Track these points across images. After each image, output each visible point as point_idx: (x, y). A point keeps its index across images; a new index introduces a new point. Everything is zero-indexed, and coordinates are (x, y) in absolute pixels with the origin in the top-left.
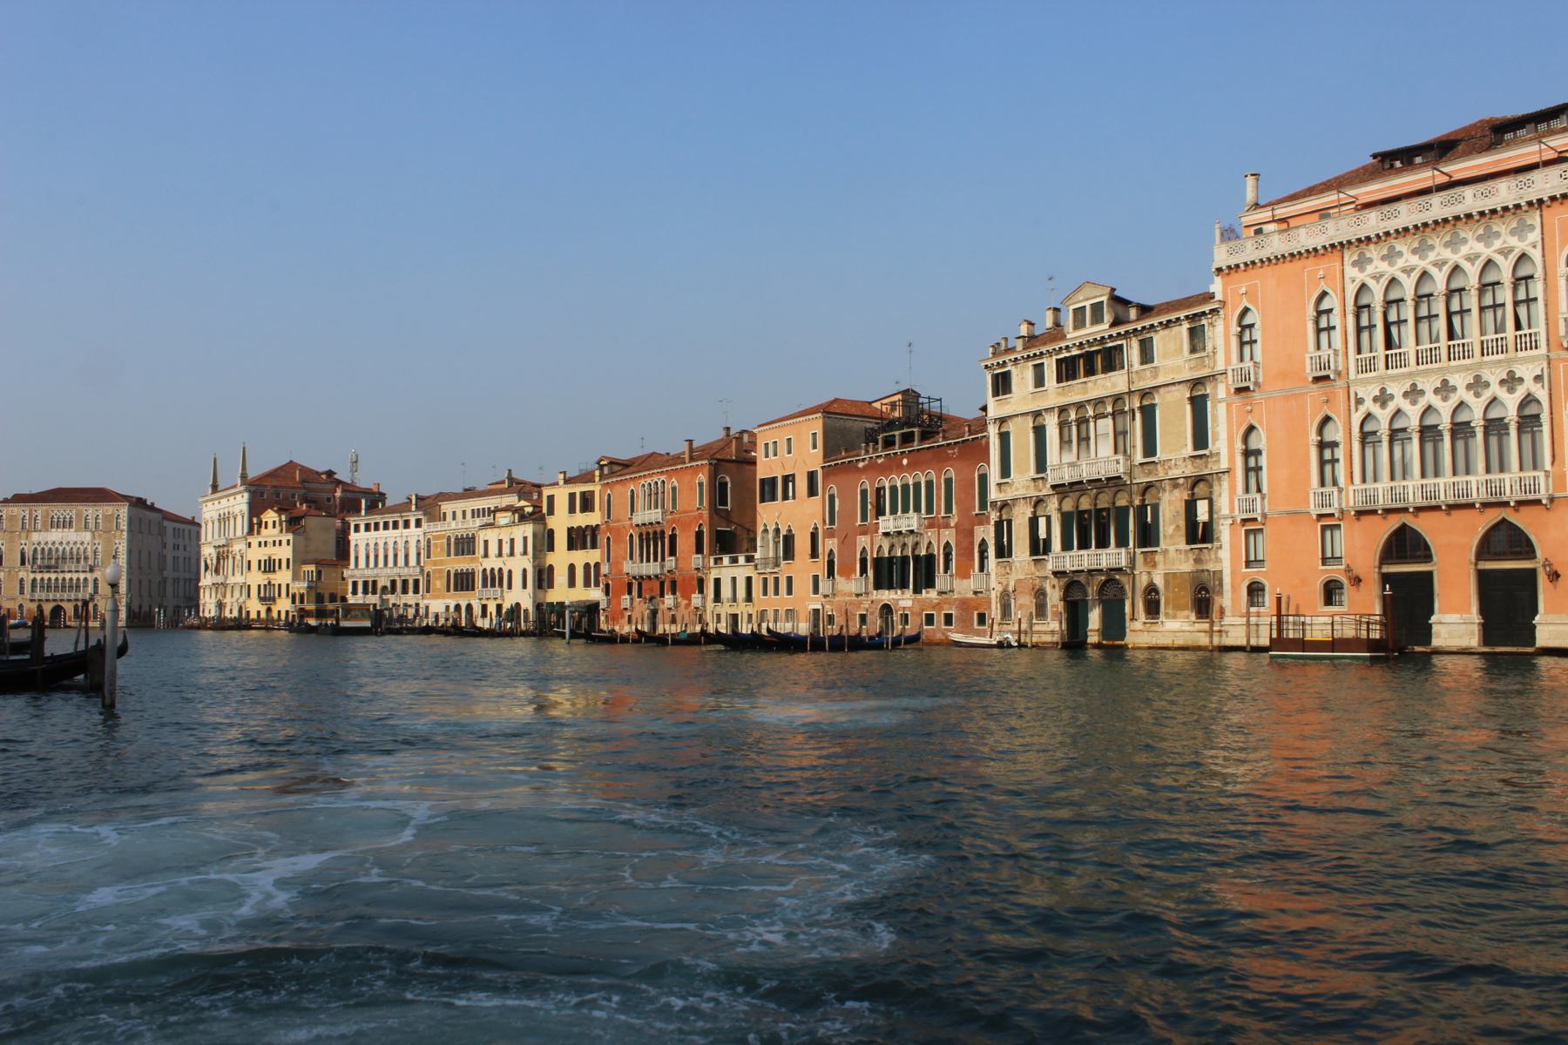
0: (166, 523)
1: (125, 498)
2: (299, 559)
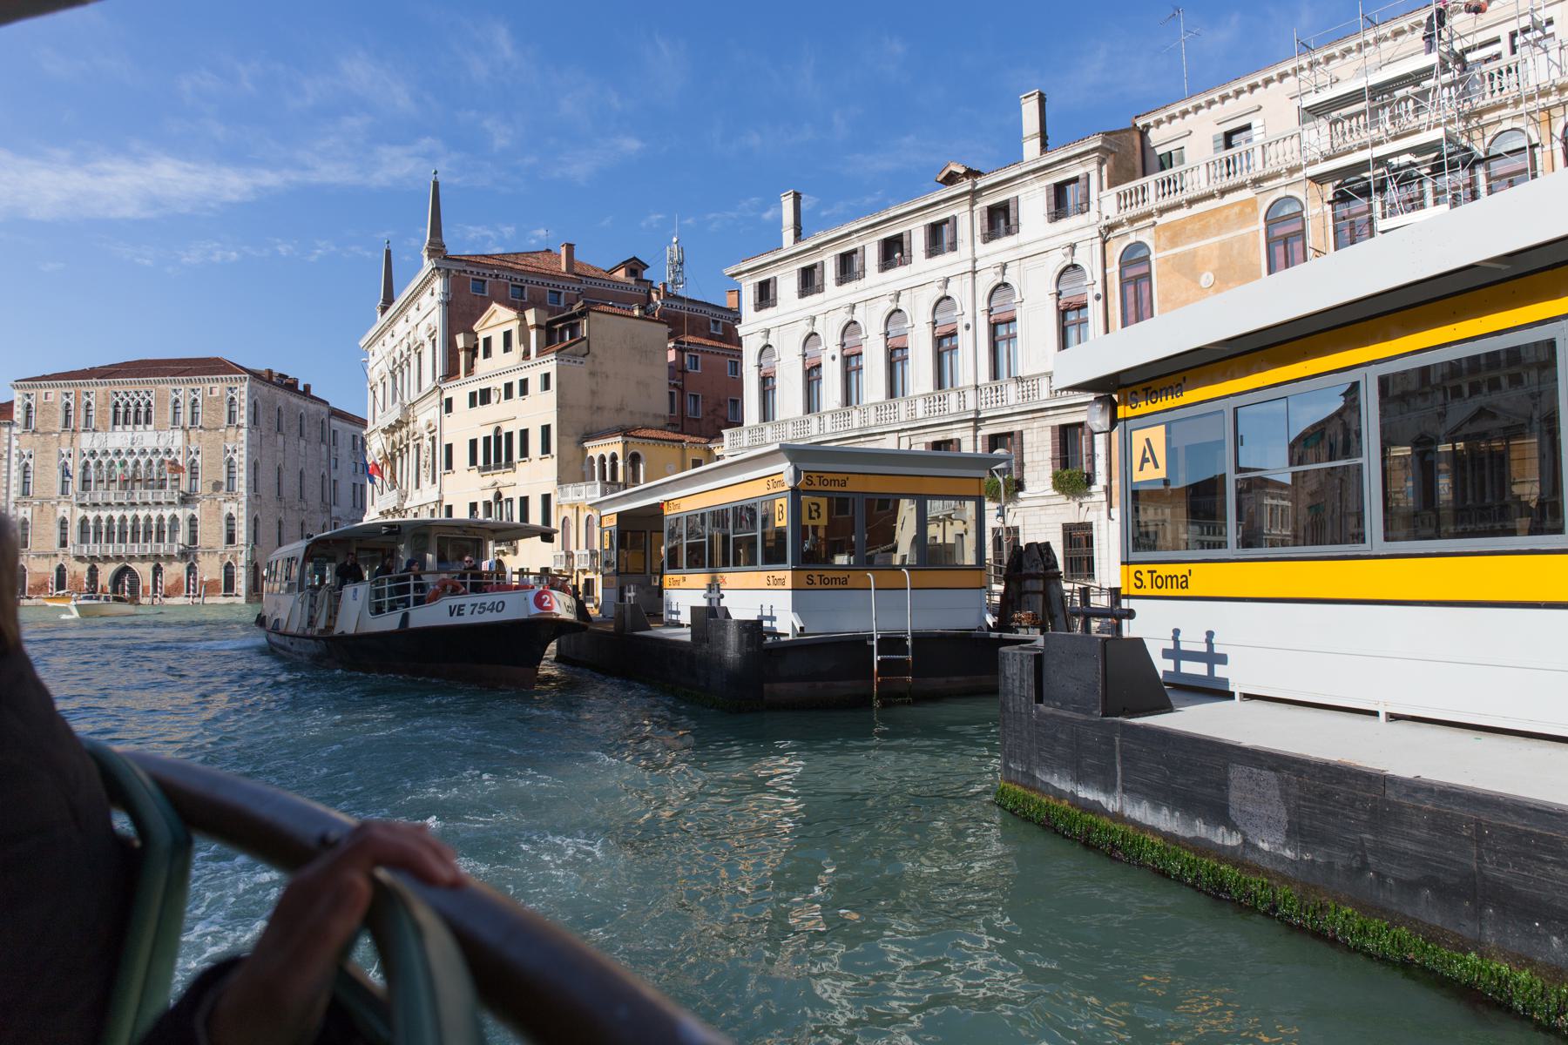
0: (336, 423)
1: (256, 375)
2: (576, 429)
